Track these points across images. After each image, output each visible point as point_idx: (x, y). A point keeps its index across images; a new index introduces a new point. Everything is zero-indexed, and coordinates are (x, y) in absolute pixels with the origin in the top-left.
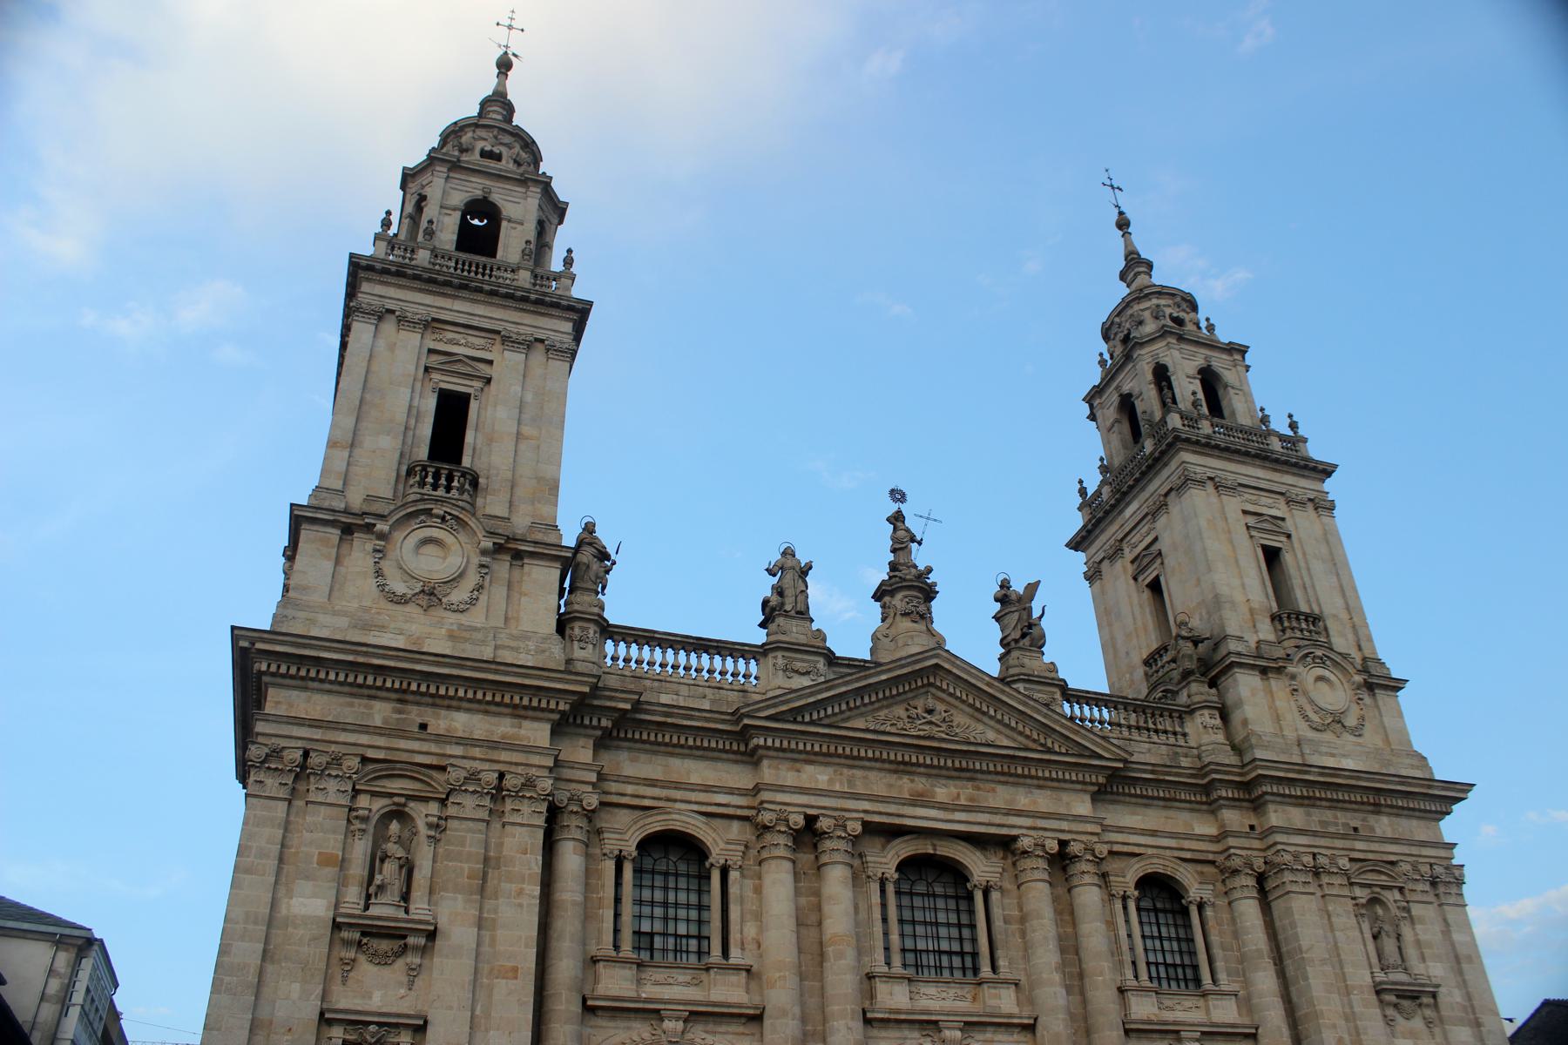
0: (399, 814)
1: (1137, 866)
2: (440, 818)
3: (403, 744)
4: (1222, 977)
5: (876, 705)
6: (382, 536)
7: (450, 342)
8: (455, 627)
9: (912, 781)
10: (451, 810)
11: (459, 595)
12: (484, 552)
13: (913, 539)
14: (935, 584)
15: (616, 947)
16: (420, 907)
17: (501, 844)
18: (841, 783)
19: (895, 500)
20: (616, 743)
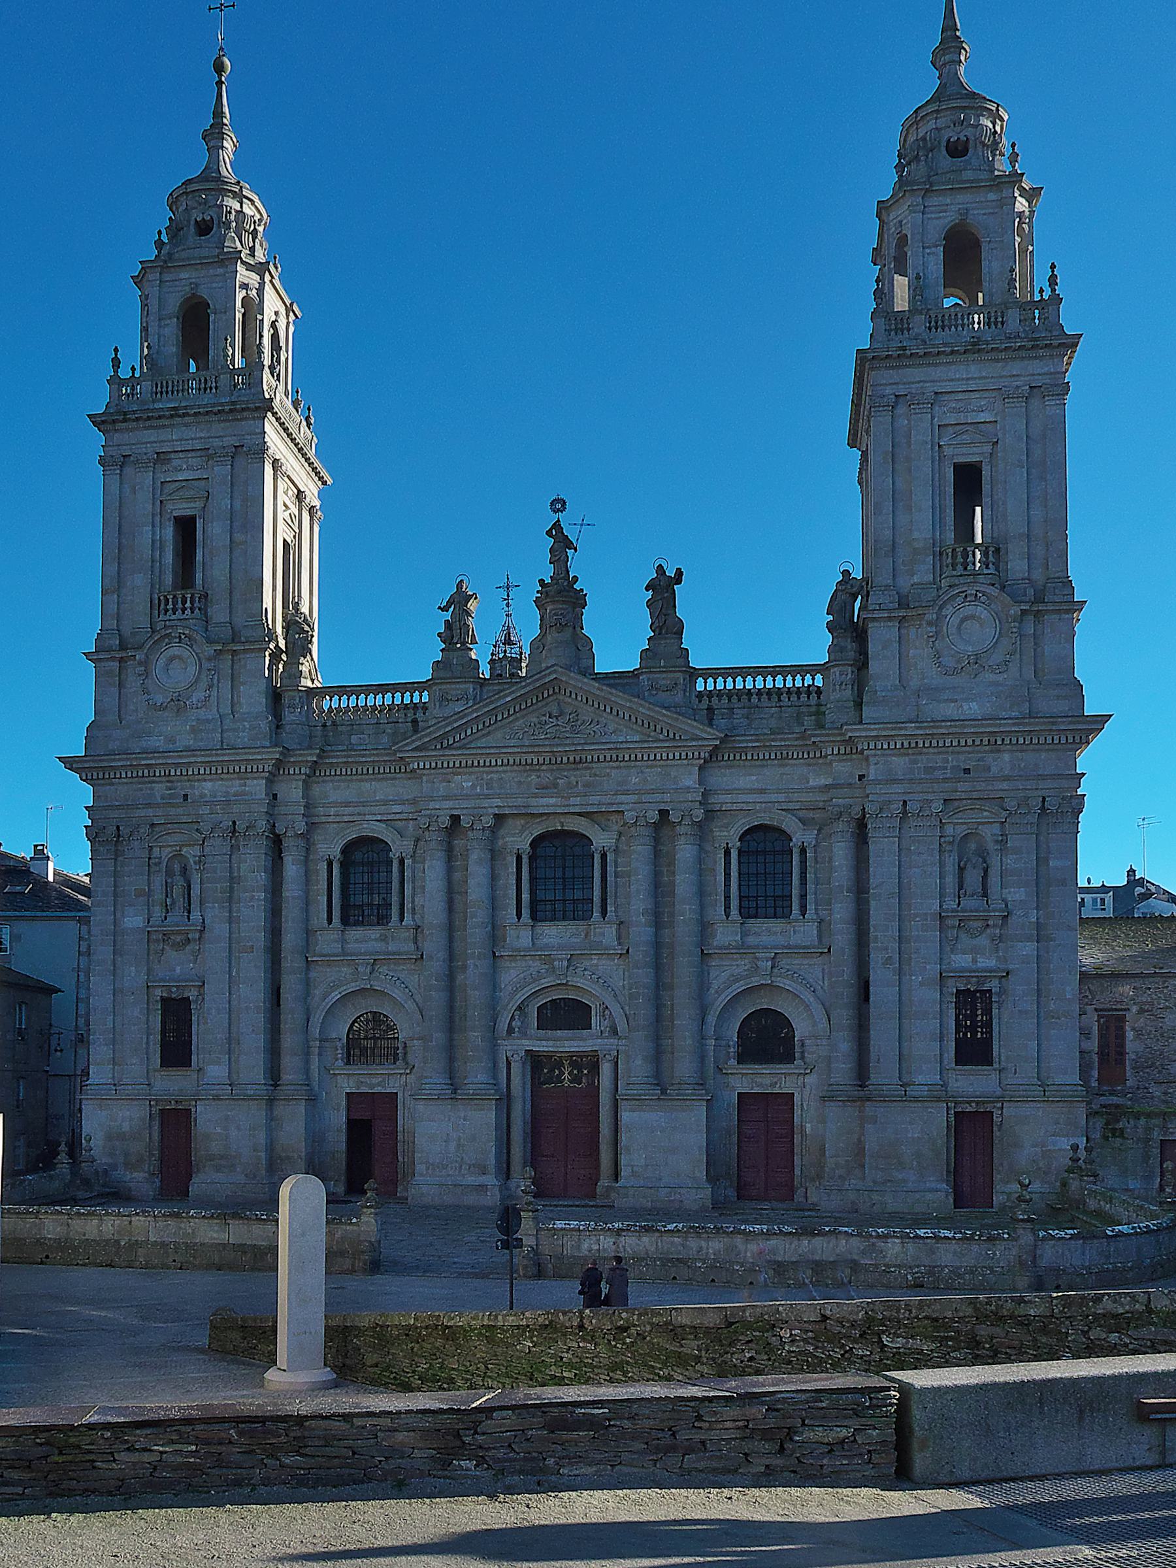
0: (178, 856)
1: (744, 821)
2: (200, 857)
3: (172, 811)
4: (810, 907)
5: (511, 718)
6: (140, 663)
7: (178, 469)
8: (194, 723)
9: (539, 777)
10: (207, 850)
11: (199, 695)
12: (209, 659)
13: (569, 544)
14: (582, 590)
15: (330, 920)
16: (196, 915)
17: (239, 869)
18: (482, 787)
19: (556, 511)
20: (321, 779)
